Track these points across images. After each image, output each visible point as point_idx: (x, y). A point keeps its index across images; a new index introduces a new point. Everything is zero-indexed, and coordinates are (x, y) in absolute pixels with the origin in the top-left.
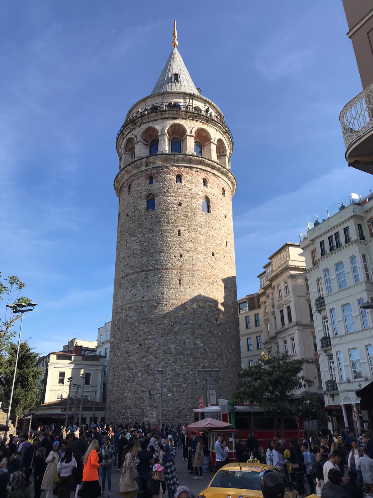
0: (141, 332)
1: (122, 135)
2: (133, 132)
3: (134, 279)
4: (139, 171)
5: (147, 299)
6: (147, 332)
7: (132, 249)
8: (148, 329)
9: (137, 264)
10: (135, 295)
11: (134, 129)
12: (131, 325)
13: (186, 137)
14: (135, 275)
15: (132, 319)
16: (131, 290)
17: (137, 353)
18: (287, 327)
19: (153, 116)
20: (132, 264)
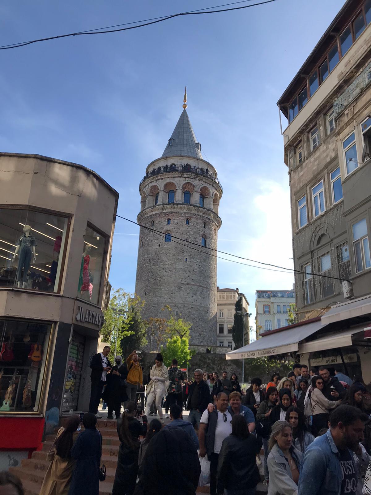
0: (200, 326)
1: (181, 174)
2: (193, 180)
3: (195, 289)
4: (198, 214)
5: (203, 306)
6: (203, 327)
7: (192, 267)
8: (204, 325)
9: (197, 280)
10: (196, 301)
11: (195, 179)
12: (194, 320)
13: (217, 204)
14: (196, 287)
15: (194, 316)
16: (193, 296)
17: (198, 339)
18: (225, 335)
19: (209, 181)
20: (193, 278)
